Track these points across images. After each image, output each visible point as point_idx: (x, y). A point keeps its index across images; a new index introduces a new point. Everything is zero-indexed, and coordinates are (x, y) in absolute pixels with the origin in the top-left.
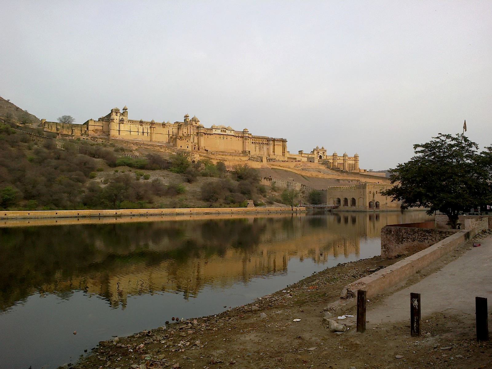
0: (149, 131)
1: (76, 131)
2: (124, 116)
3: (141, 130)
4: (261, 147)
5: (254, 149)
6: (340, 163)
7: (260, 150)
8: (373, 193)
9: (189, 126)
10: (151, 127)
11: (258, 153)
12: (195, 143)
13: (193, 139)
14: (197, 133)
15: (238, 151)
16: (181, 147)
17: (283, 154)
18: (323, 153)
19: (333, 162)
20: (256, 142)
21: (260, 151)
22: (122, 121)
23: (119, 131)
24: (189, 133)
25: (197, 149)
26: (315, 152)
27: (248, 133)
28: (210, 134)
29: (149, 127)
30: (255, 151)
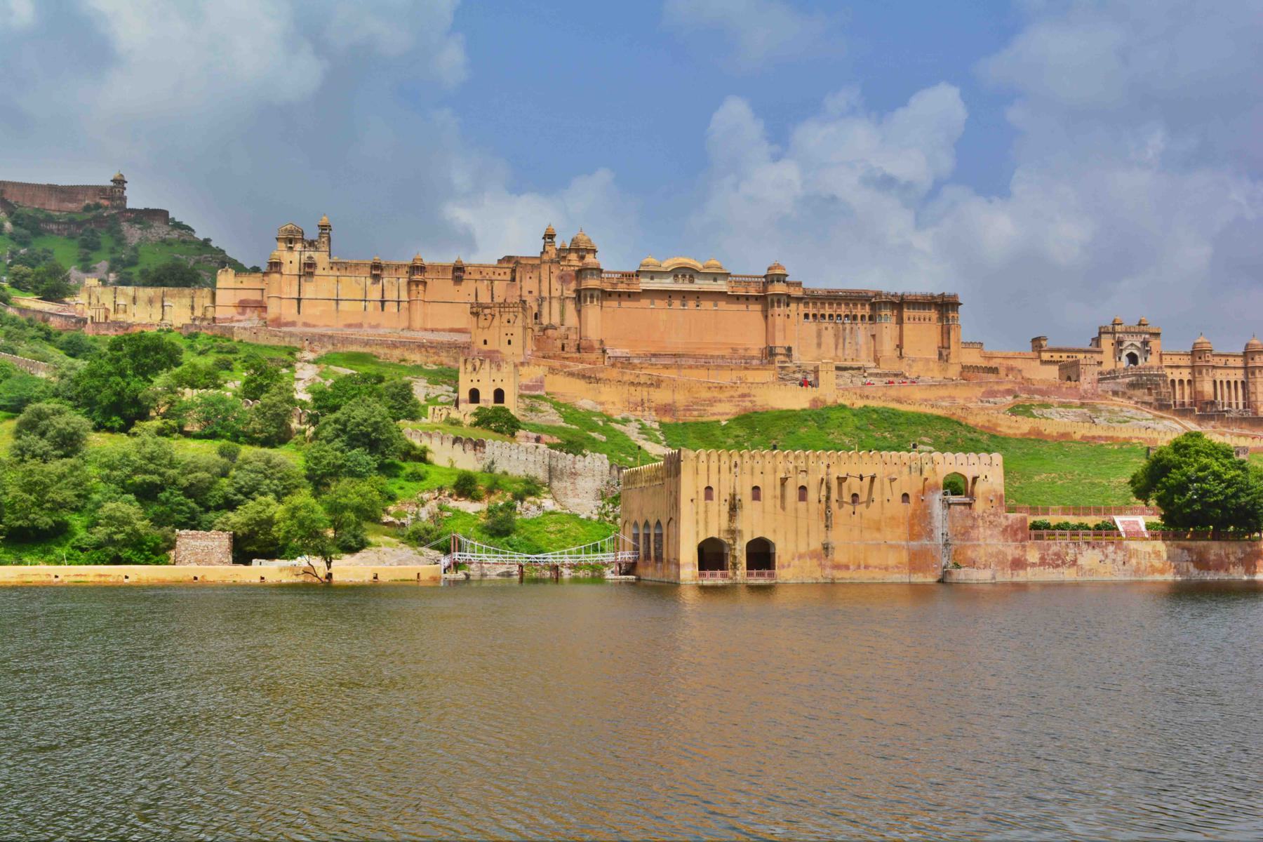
0: (404, 296)
1: (175, 308)
2: (317, 249)
3: (375, 293)
4: (844, 330)
5: (815, 341)
6: (1228, 382)
7: (841, 341)
8: (733, 497)
9: (547, 267)
10: (409, 283)
11: (832, 353)
12: (569, 329)
13: (562, 313)
14: (578, 291)
15: (746, 350)
16: (485, 342)
17: (940, 354)
18: (1145, 343)
19: (1190, 377)
20: (822, 312)
21: (841, 346)
22: (308, 269)
23: (299, 300)
24: (545, 294)
25: (574, 350)
26: (1107, 342)
27: (787, 279)
28: (630, 295)
29: (403, 281)
30: (819, 345)
